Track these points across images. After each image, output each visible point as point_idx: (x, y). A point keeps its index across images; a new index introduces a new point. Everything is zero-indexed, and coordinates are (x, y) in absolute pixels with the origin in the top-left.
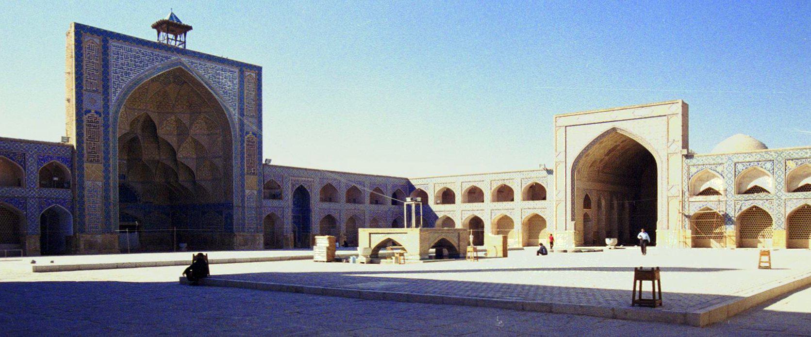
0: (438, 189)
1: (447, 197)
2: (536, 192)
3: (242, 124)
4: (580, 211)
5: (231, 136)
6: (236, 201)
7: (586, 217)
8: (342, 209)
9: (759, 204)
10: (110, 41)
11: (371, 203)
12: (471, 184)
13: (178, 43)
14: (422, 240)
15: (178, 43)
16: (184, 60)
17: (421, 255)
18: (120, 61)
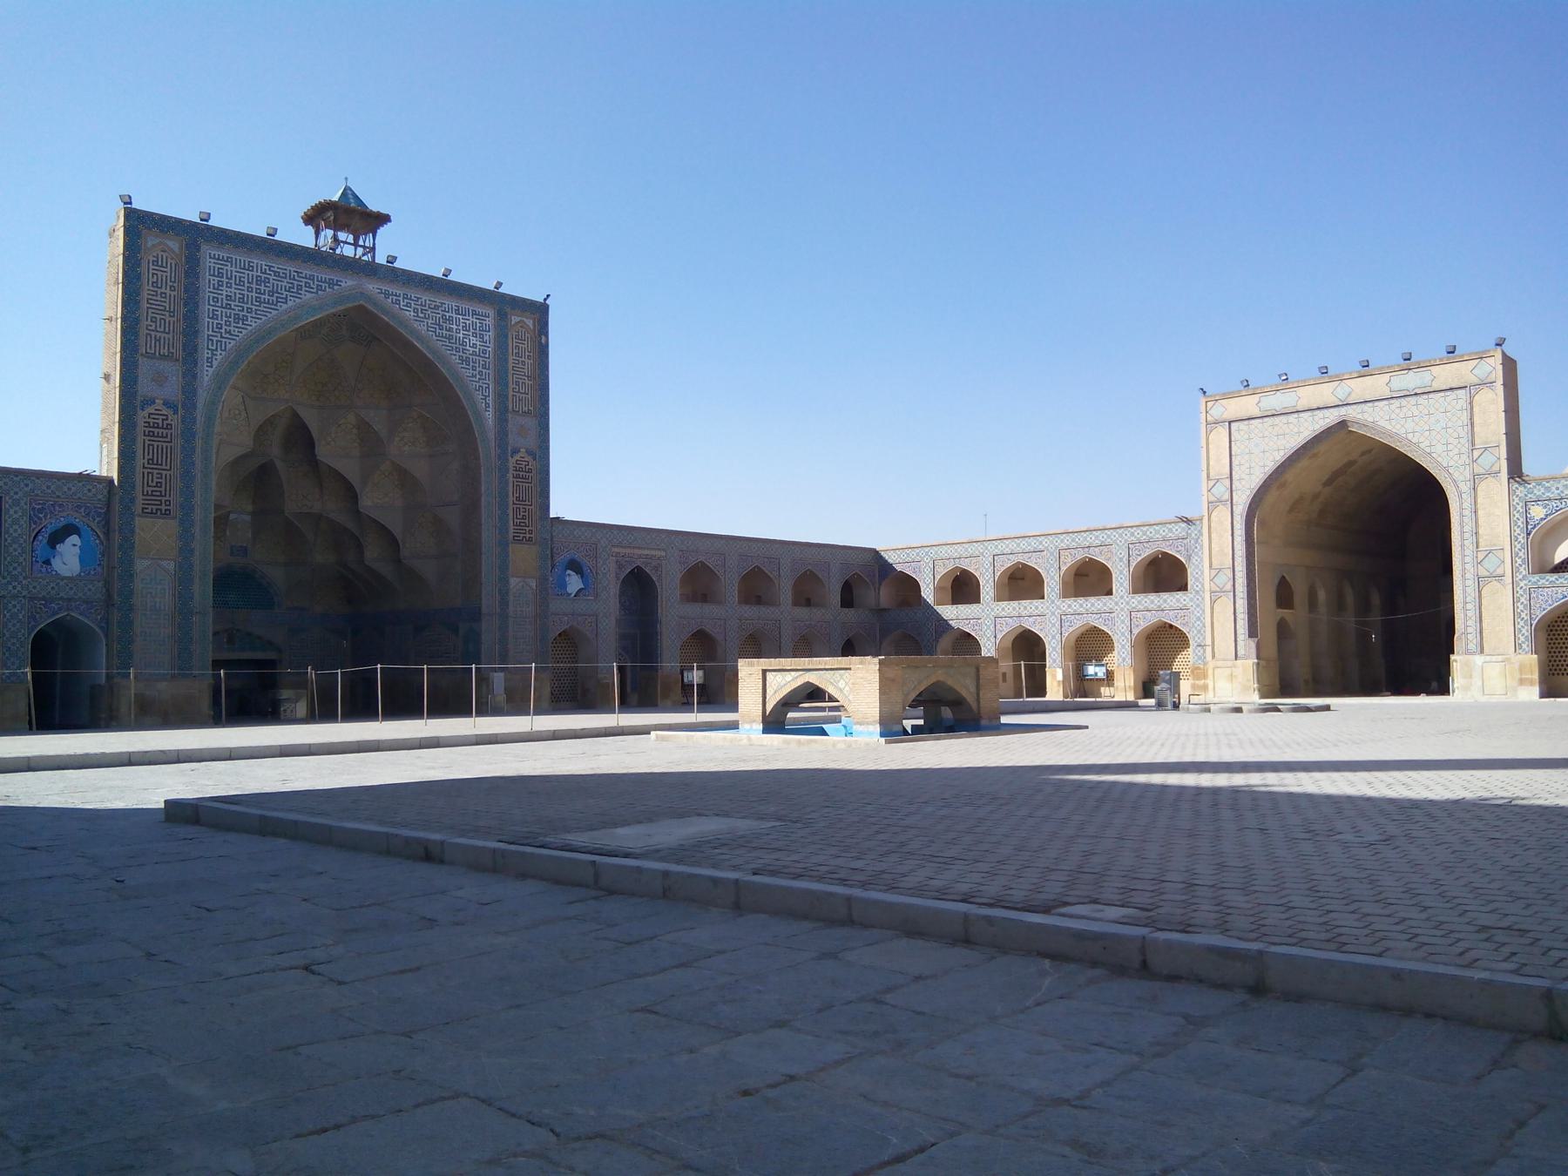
0: (942, 571)
1: (963, 587)
2: (1164, 573)
3: (502, 432)
4: (1270, 614)
5: (477, 458)
6: (488, 602)
7: (1283, 631)
8: (726, 615)
11: (796, 603)
12: (1014, 559)
15: (360, 251)
16: (372, 287)
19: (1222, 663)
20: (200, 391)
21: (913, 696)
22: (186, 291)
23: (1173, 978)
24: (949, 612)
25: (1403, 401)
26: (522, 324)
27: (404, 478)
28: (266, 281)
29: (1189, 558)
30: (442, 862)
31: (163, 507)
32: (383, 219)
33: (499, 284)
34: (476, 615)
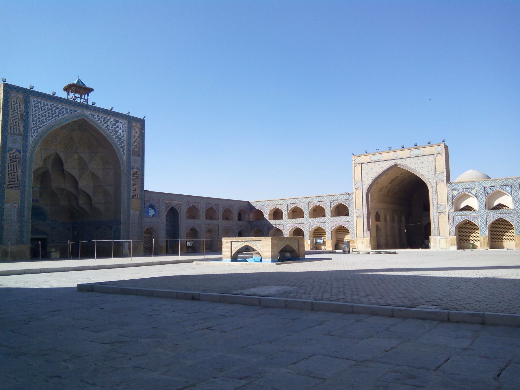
0: (271, 209)
1: (277, 214)
2: (341, 210)
3: (129, 162)
5: (120, 170)
6: (123, 219)
7: (378, 228)
8: (201, 223)
9: (504, 217)
10: (31, 98)
13: (82, 100)
14: (273, 246)
15: (82, 100)
16: (87, 112)
17: (272, 258)
18: (38, 112)
19: (360, 238)
20: (28, 146)
21: (280, 250)
22: (25, 112)
23: (457, 322)
24: (273, 222)
25: (415, 158)
26: (136, 126)
27: (94, 176)
28: (52, 110)
29: (349, 205)
30: (199, 300)
31: (15, 186)
32: (91, 90)
33: (129, 113)
34: (119, 223)
